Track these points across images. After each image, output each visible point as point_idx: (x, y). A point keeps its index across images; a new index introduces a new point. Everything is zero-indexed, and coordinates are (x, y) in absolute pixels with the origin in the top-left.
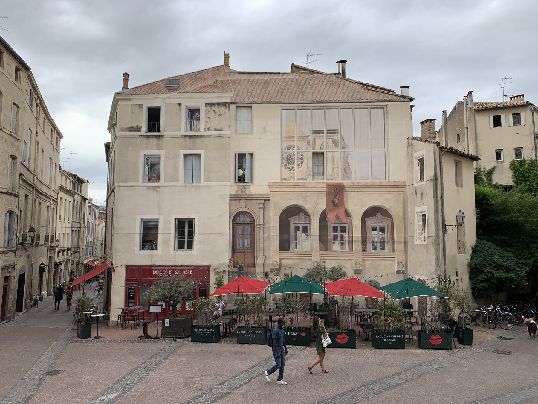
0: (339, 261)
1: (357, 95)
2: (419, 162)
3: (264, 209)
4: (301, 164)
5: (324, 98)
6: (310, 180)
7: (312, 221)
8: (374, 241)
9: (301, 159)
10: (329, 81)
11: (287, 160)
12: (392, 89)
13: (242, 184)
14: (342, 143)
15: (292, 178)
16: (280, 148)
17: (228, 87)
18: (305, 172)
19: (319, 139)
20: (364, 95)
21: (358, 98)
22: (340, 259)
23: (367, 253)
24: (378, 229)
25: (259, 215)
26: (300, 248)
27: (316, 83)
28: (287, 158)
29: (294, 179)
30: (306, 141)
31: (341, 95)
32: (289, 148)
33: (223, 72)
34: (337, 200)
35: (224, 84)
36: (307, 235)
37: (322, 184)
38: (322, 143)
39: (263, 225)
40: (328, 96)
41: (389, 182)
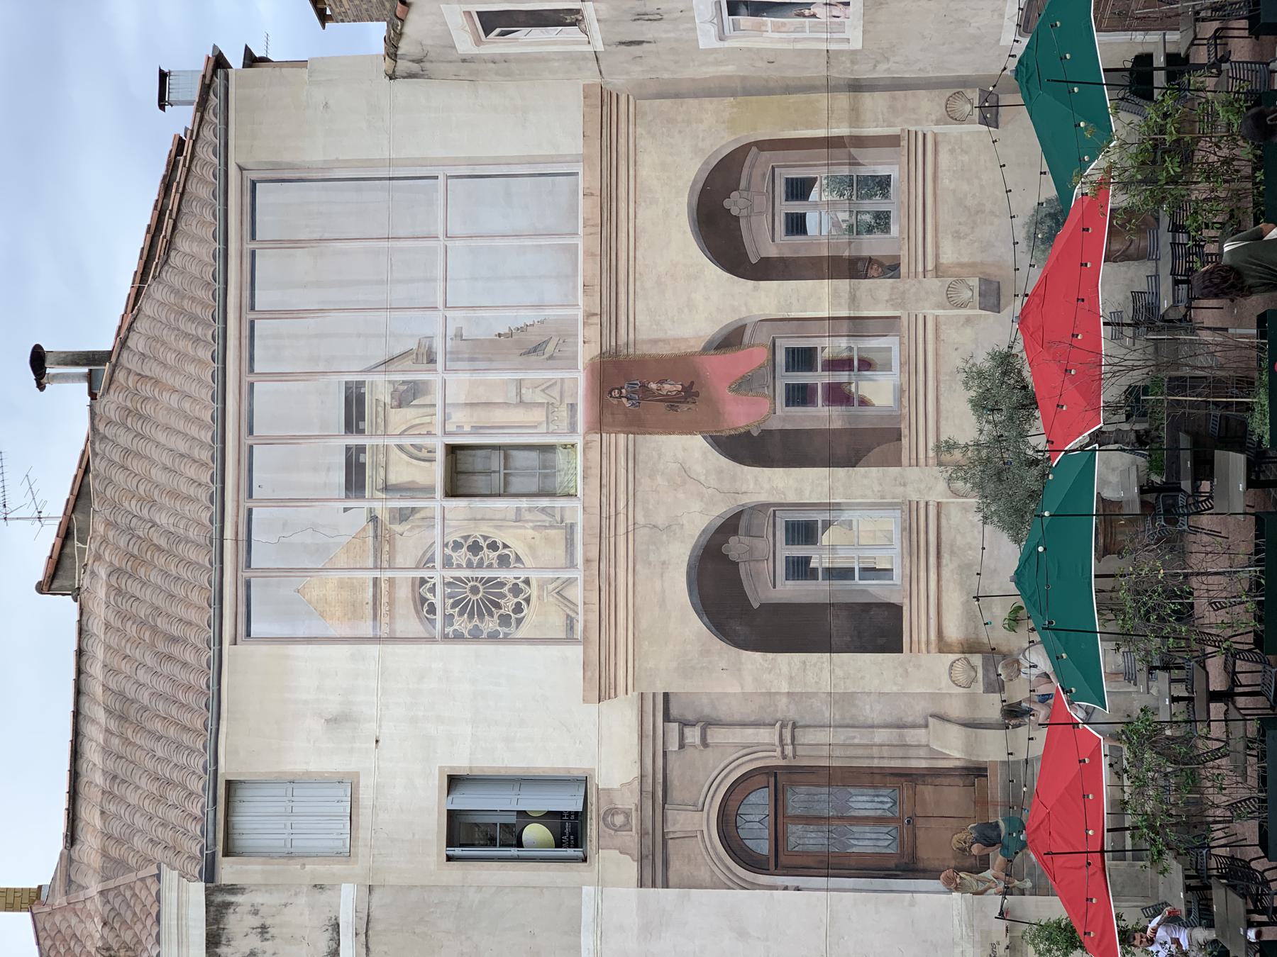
0: (943, 378)
1: (193, 299)
2: (498, 30)
3: (708, 724)
4: (501, 551)
5: (202, 444)
6: (574, 510)
7: (763, 498)
8: (851, 227)
9: (475, 548)
10: (124, 425)
11: (481, 616)
12: (168, 146)
13: (592, 828)
14: (408, 363)
15: (564, 593)
16: (425, 649)
17: (135, 895)
20: (194, 269)
21: (205, 295)
22: (937, 372)
25: (736, 745)
26: (890, 556)
28: (471, 616)
29: (570, 582)
30: (397, 528)
31: (191, 369)
32: (424, 606)
33: (64, 919)
34: (667, 387)
35: (119, 914)
36: (827, 525)
37: (595, 455)
38: (404, 456)
39: (782, 727)
40: (193, 431)
41: (585, 159)
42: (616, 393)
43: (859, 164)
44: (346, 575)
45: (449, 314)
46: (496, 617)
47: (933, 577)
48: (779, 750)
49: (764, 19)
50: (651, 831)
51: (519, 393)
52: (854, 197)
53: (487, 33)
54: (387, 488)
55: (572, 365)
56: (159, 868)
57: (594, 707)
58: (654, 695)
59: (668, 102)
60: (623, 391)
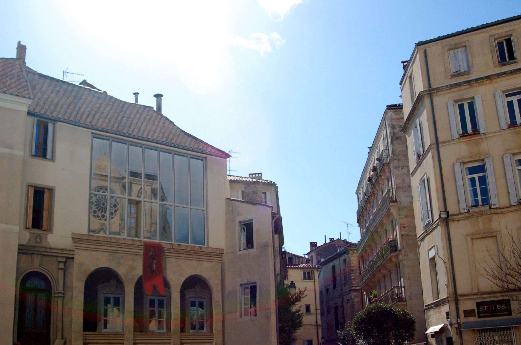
1: (177, 139)
2: (245, 227)
3: (65, 270)
4: (114, 213)
5: (143, 134)
7: (126, 291)
11: (96, 205)
13: (36, 231)
15: (102, 230)
17: (25, 90)
18: (118, 224)
23: (186, 334)
24: (197, 304)
27: (133, 113)
28: (96, 202)
30: (121, 184)
31: (161, 136)
32: (101, 188)
33: (18, 68)
34: (155, 265)
36: (119, 310)
37: (138, 243)
41: (208, 247)
42: (153, 251)
43: (207, 322)
44: (109, 168)
45: (173, 207)
46: (96, 210)
48: (57, 292)
49: (249, 295)
50: (34, 250)
51: (154, 224)
52: (199, 320)
53: (243, 224)
55: (161, 239)
56: (32, 99)
57: (70, 235)
58: (74, 254)
59: (220, 271)
60: (154, 253)
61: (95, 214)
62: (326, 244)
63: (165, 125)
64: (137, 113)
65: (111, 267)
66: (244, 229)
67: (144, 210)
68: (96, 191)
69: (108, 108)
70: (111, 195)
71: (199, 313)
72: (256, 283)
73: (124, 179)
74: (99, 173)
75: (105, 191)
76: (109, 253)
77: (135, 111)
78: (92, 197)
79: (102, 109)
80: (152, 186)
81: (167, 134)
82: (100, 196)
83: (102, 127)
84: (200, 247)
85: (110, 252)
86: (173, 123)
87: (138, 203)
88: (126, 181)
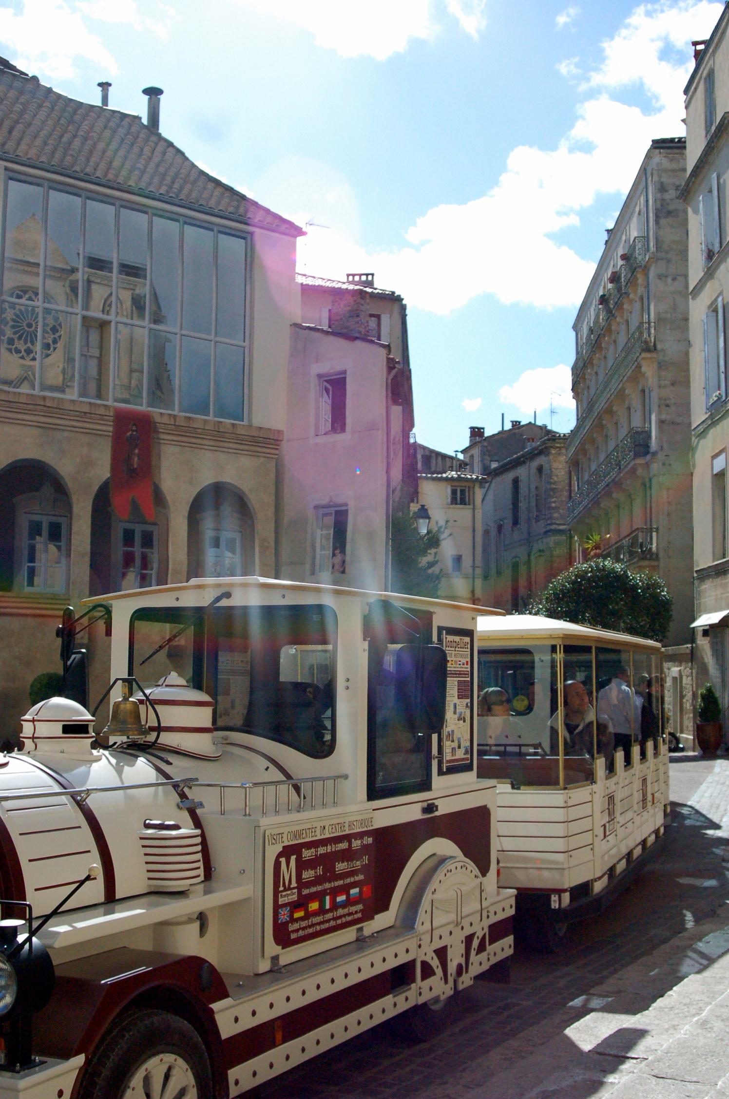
1: (191, 191)
2: (330, 387)
5: (117, 176)
6: (72, 394)
7: (75, 509)
9: (54, 330)
10: (128, 133)
11: (13, 327)
14: (154, 308)
15: (26, 382)
19: (98, 283)
28: (13, 320)
30: (67, 284)
31: (156, 180)
34: (136, 459)
36: (59, 548)
37: (102, 411)
41: (250, 426)
42: (134, 428)
44: (42, 247)
46: (14, 336)
47: (28, 612)
49: (332, 530)
51: (136, 371)
53: (325, 381)
54: (89, 282)
55: (150, 404)
59: (273, 476)
60: (135, 433)
61: (10, 346)
62: (502, 432)
63: (167, 157)
64: (105, 127)
65: (43, 459)
66: (327, 390)
67: (118, 342)
68: (15, 296)
69: (42, 115)
70: (47, 305)
71: (227, 562)
72: (346, 505)
73: (74, 272)
74: (20, 257)
75: (33, 297)
76: (39, 430)
77: (101, 123)
78: (6, 310)
79: (27, 117)
80: (134, 290)
81: (168, 179)
82: (23, 308)
83: (29, 156)
84: (233, 425)
85: (43, 427)
86: (183, 154)
87: (103, 325)
88: (79, 276)
